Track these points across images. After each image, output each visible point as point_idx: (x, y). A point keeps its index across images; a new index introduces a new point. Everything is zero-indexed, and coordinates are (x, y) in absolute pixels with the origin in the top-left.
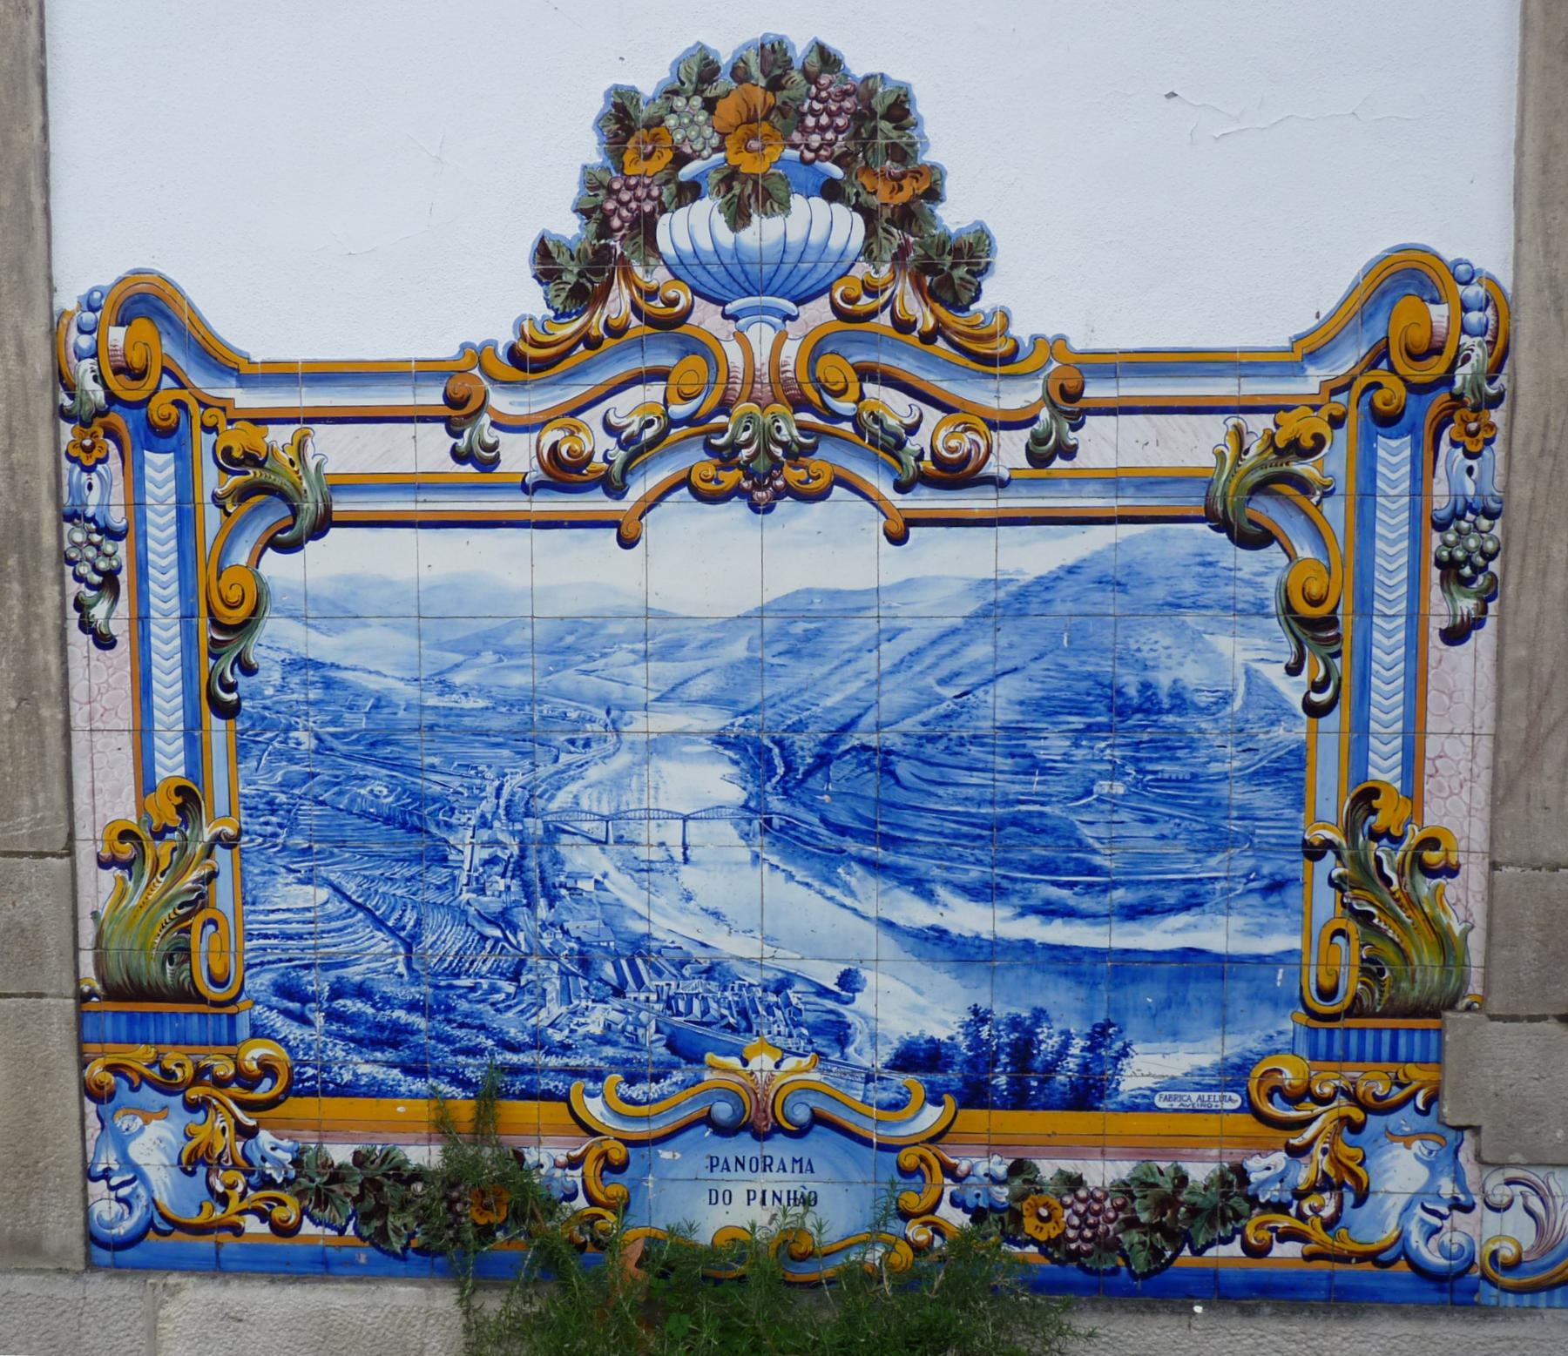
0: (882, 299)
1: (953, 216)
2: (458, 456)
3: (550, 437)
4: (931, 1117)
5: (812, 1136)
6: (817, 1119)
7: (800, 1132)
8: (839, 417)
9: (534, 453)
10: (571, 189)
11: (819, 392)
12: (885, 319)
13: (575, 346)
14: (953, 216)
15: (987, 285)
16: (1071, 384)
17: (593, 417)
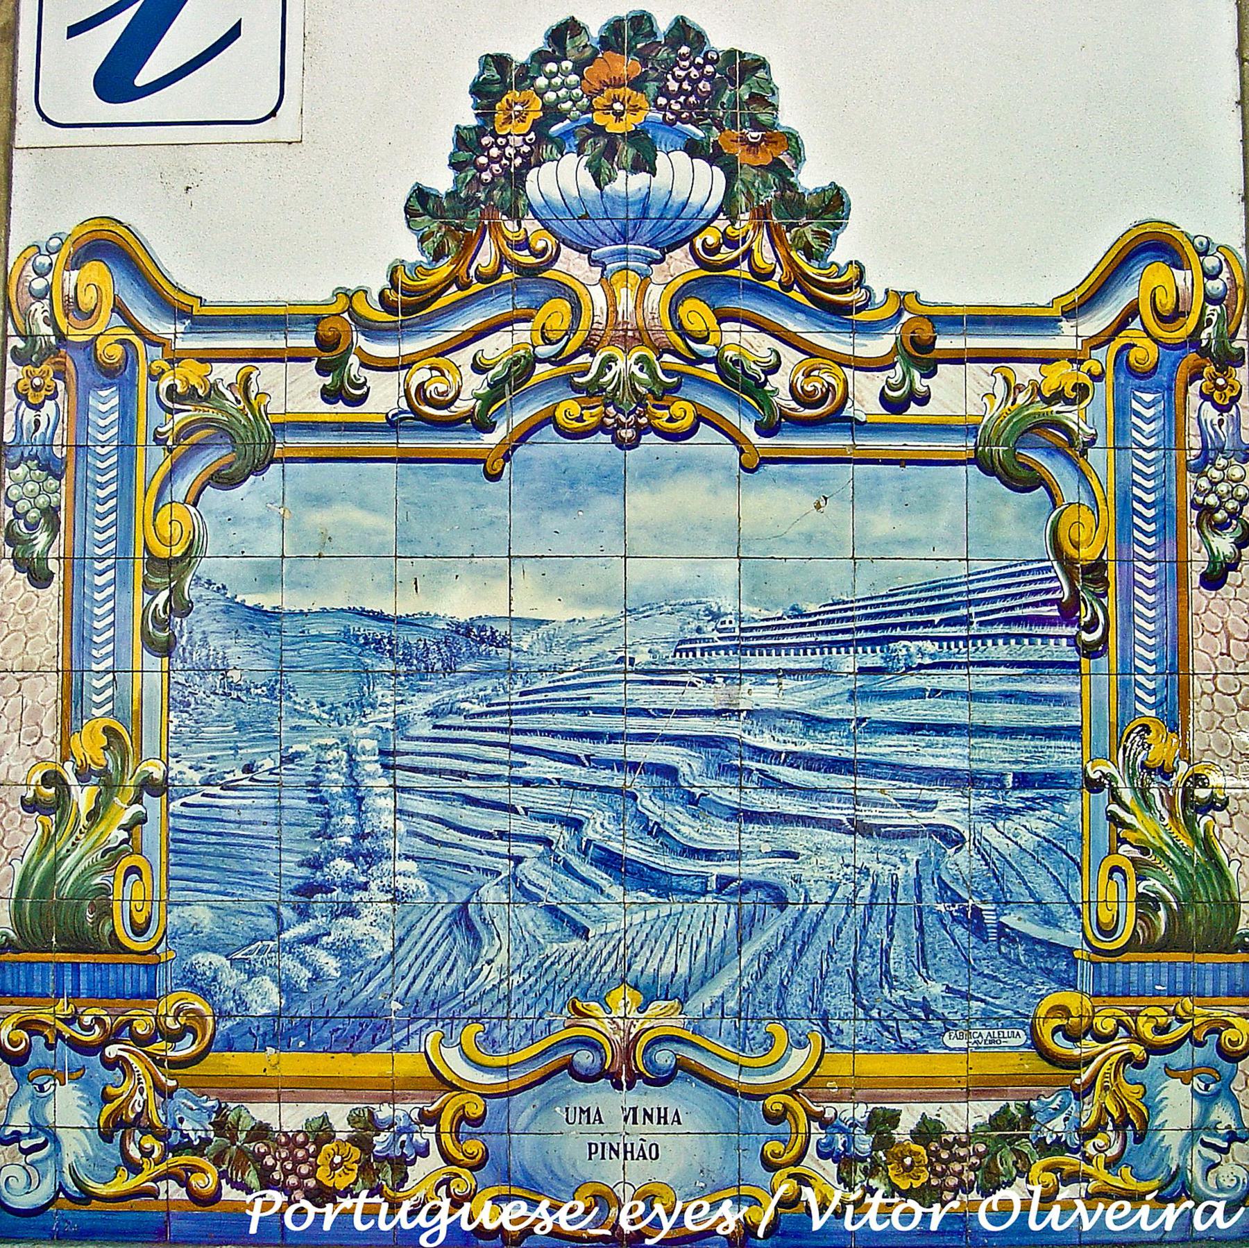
0: (742, 249)
1: (809, 179)
2: (329, 395)
3: (420, 375)
4: (797, 1063)
5: (675, 1086)
6: (682, 1068)
7: (661, 1080)
8: (701, 359)
9: (402, 394)
11: (684, 340)
12: (744, 265)
14: (809, 179)
16: (926, 334)
17: (464, 357)
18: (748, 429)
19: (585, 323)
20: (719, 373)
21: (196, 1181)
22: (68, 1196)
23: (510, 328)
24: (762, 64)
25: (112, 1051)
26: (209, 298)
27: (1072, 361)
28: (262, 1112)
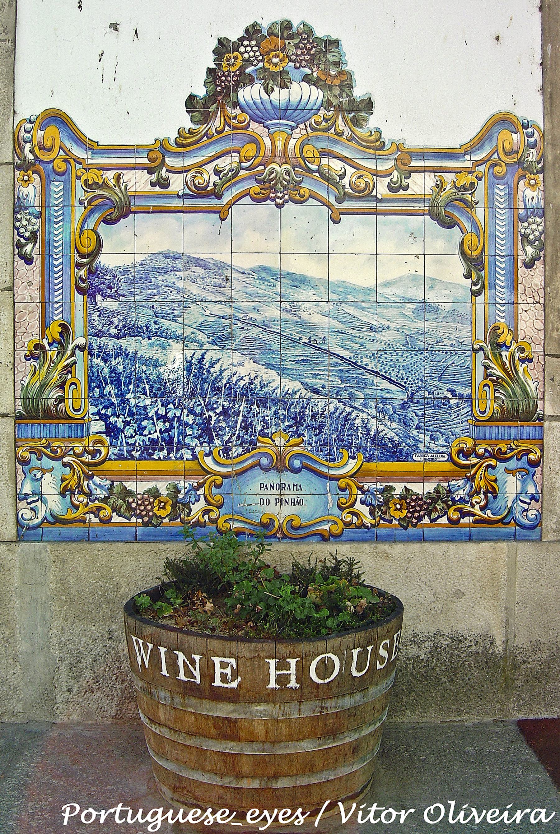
1: (358, 93)
2: (153, 184)
4: (352, 466)
9: (185, 183)
10: (203, 76)
13: (202, 138)
14: (358, 93)
15: (372, 118)
17: (210, 167)
18: (332, 200)
19: (262, 154)
20: (319, 174)
21: (102, 514)
22: (48, 522)
23: (230, 155)
24: (336, 43)
25: (66, 460)
26: (100, 144)
27: (469, 173)
28: (130, 486)
